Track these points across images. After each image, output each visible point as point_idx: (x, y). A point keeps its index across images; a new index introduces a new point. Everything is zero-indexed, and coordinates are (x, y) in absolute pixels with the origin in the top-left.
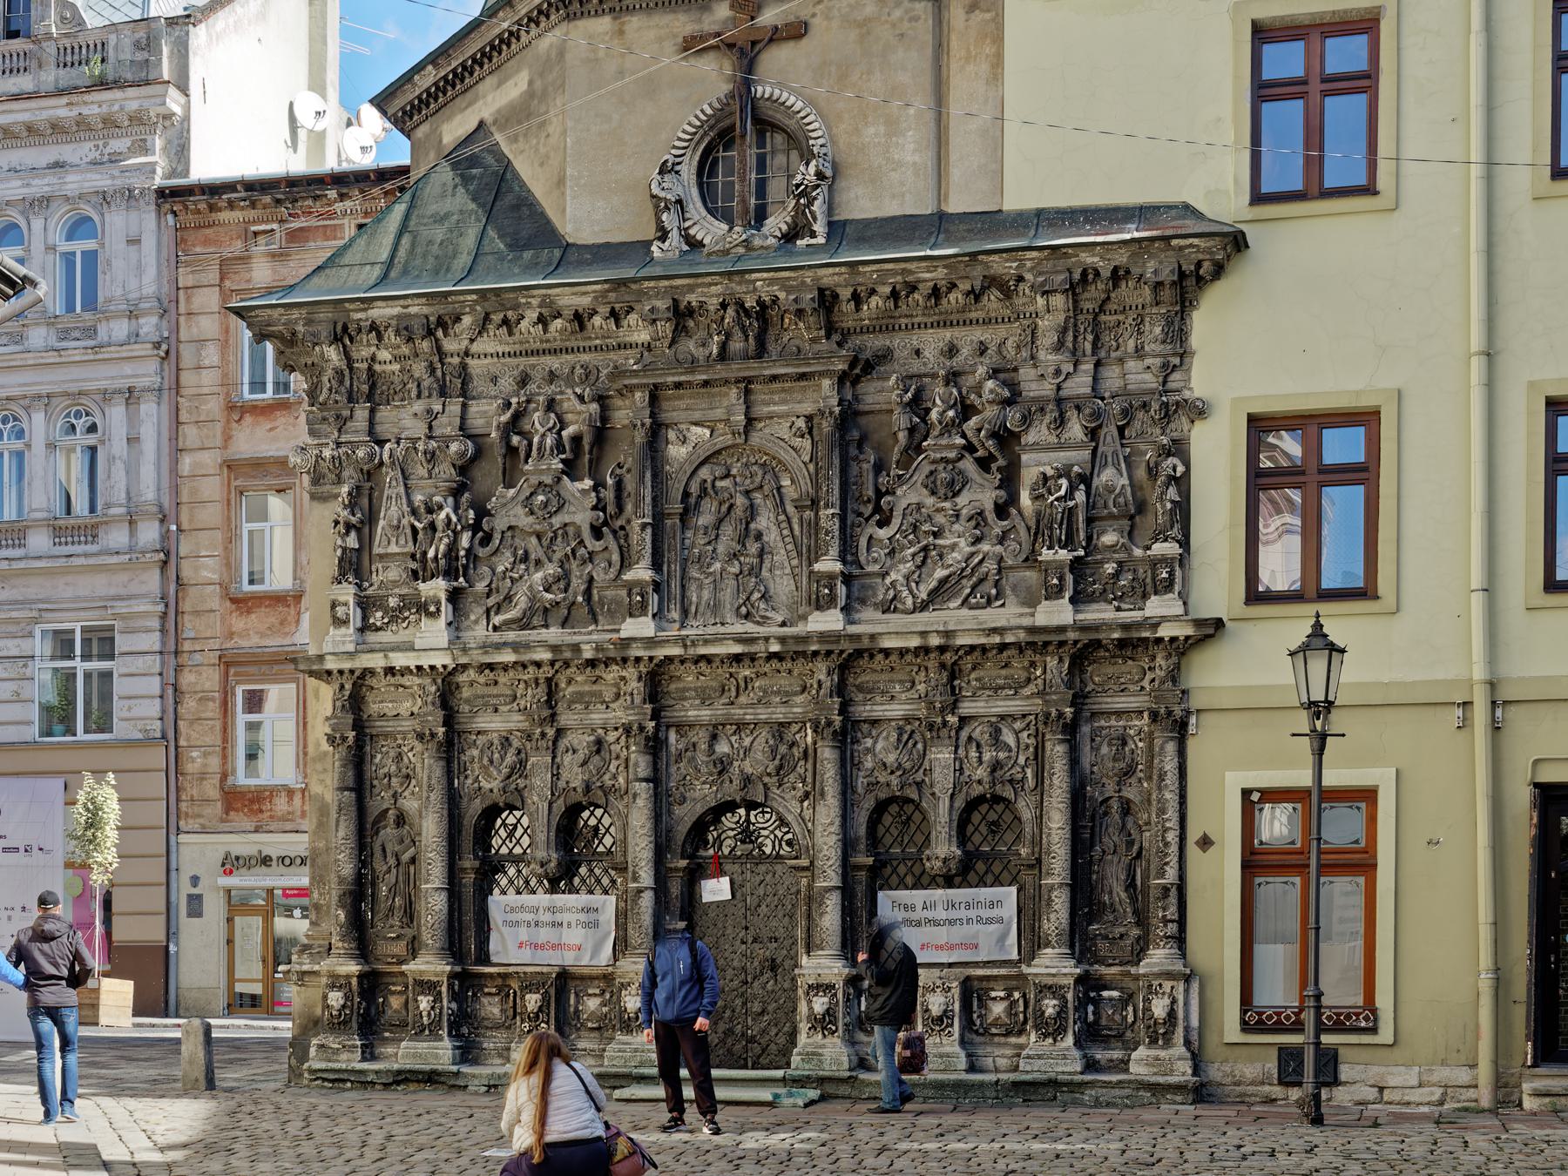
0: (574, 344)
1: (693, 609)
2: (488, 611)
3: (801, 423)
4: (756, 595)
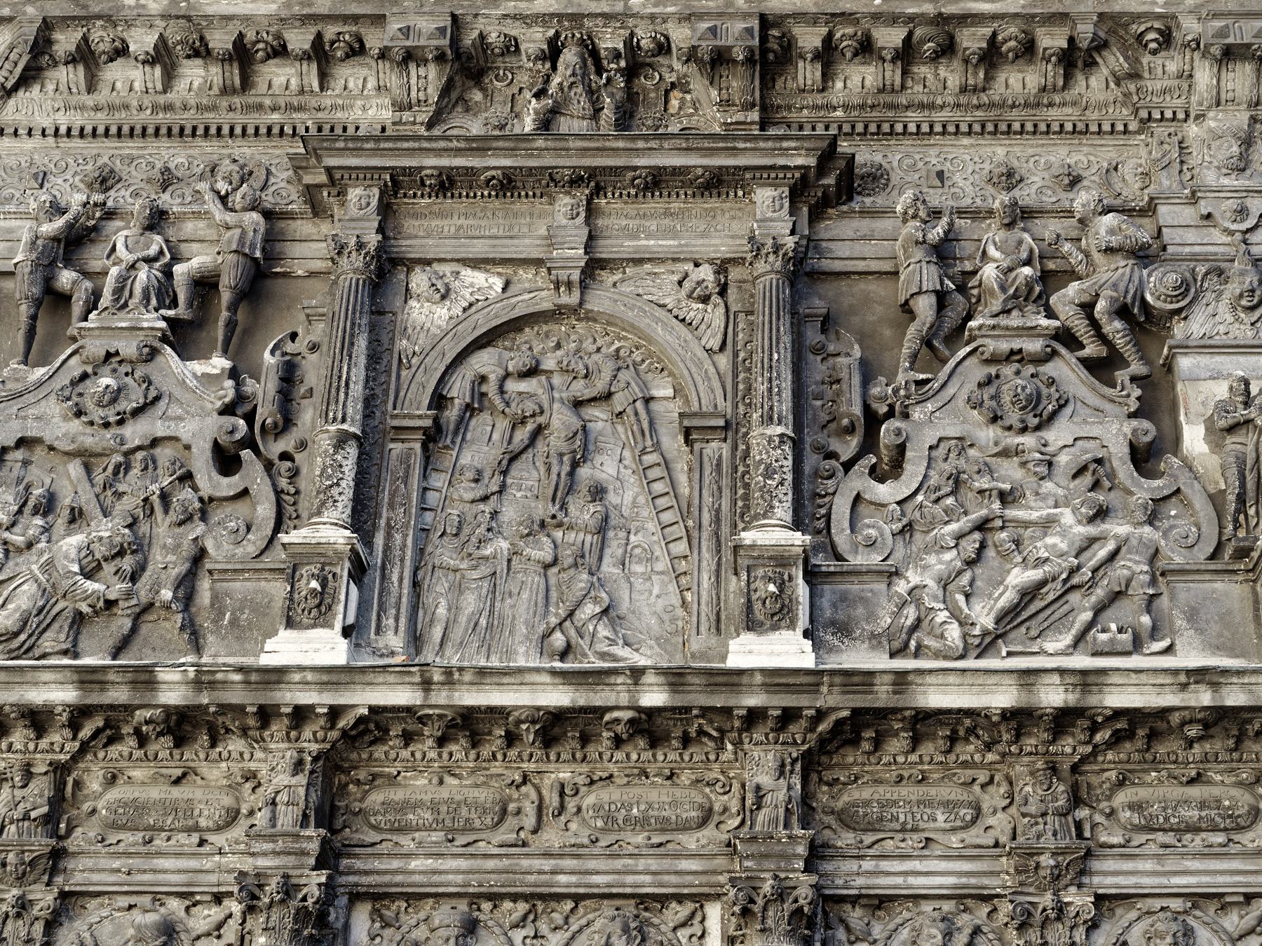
0: (222, 118)
1: (437, 632)
4: (589, 609)
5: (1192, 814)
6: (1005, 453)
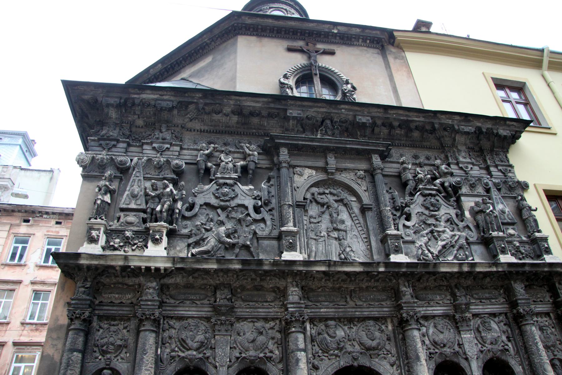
1: (313, 254)
2: (189, 245)
3: (362, 172)
5: (487, 295)
6: (432, 216)
